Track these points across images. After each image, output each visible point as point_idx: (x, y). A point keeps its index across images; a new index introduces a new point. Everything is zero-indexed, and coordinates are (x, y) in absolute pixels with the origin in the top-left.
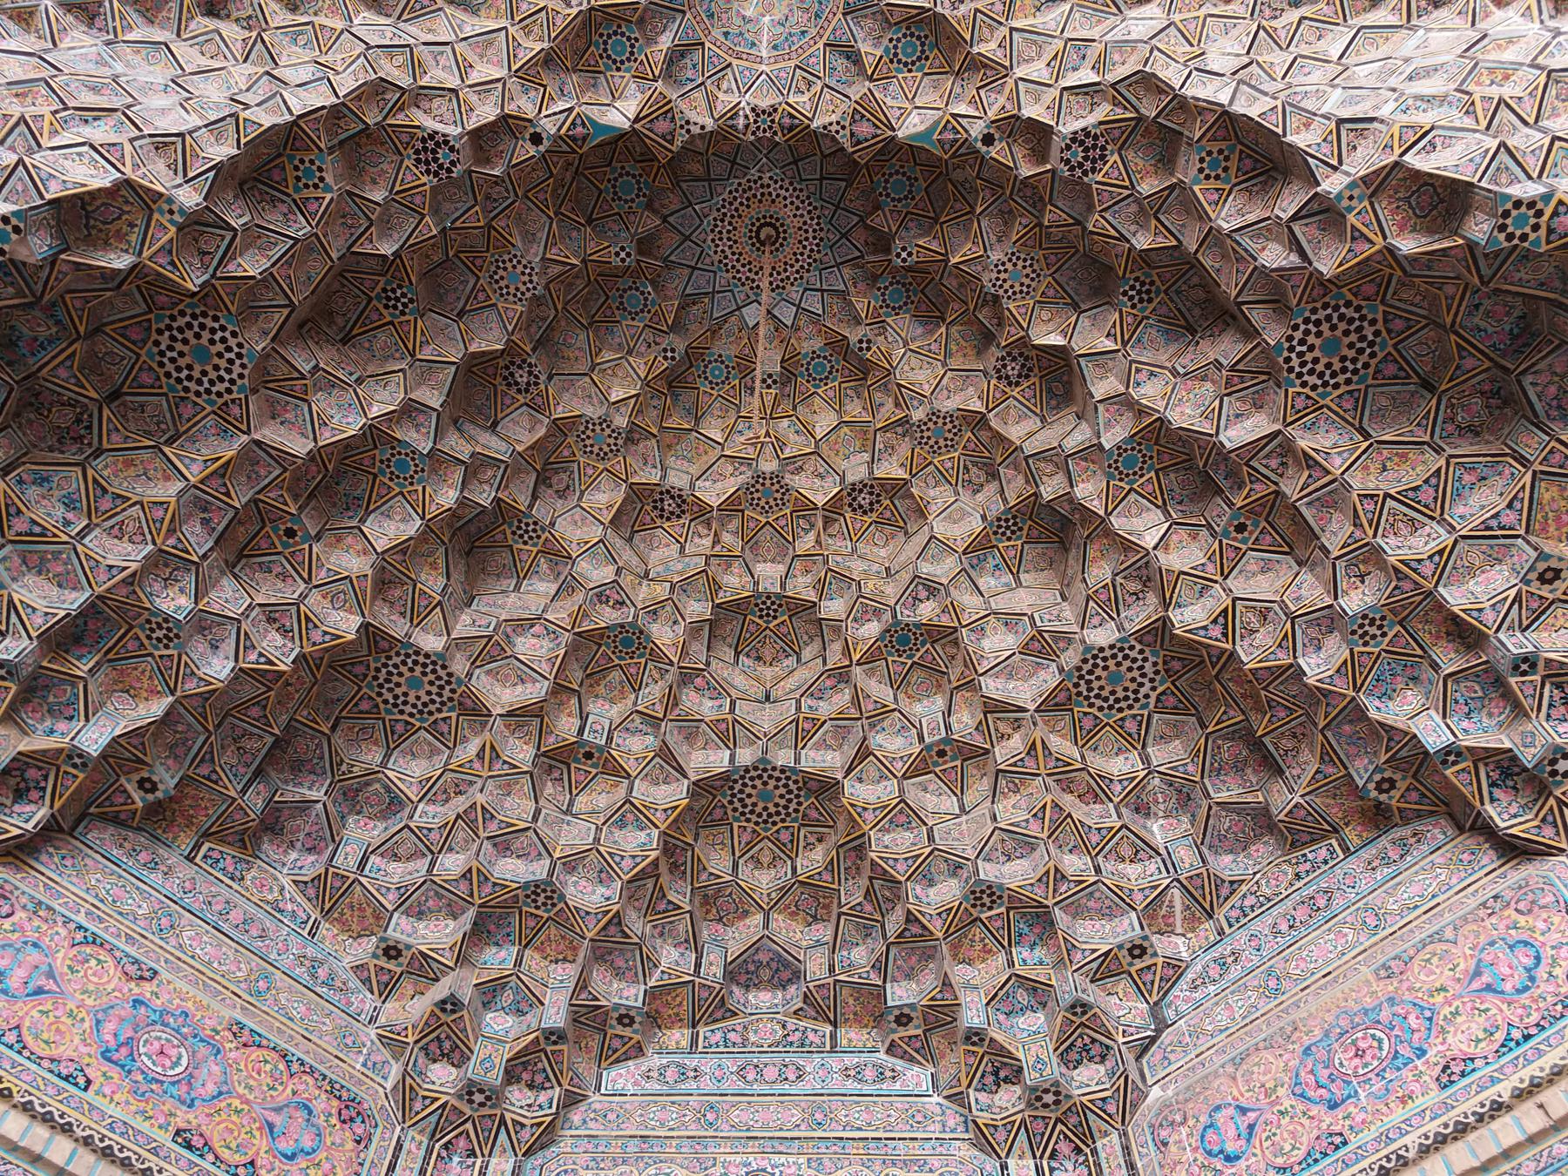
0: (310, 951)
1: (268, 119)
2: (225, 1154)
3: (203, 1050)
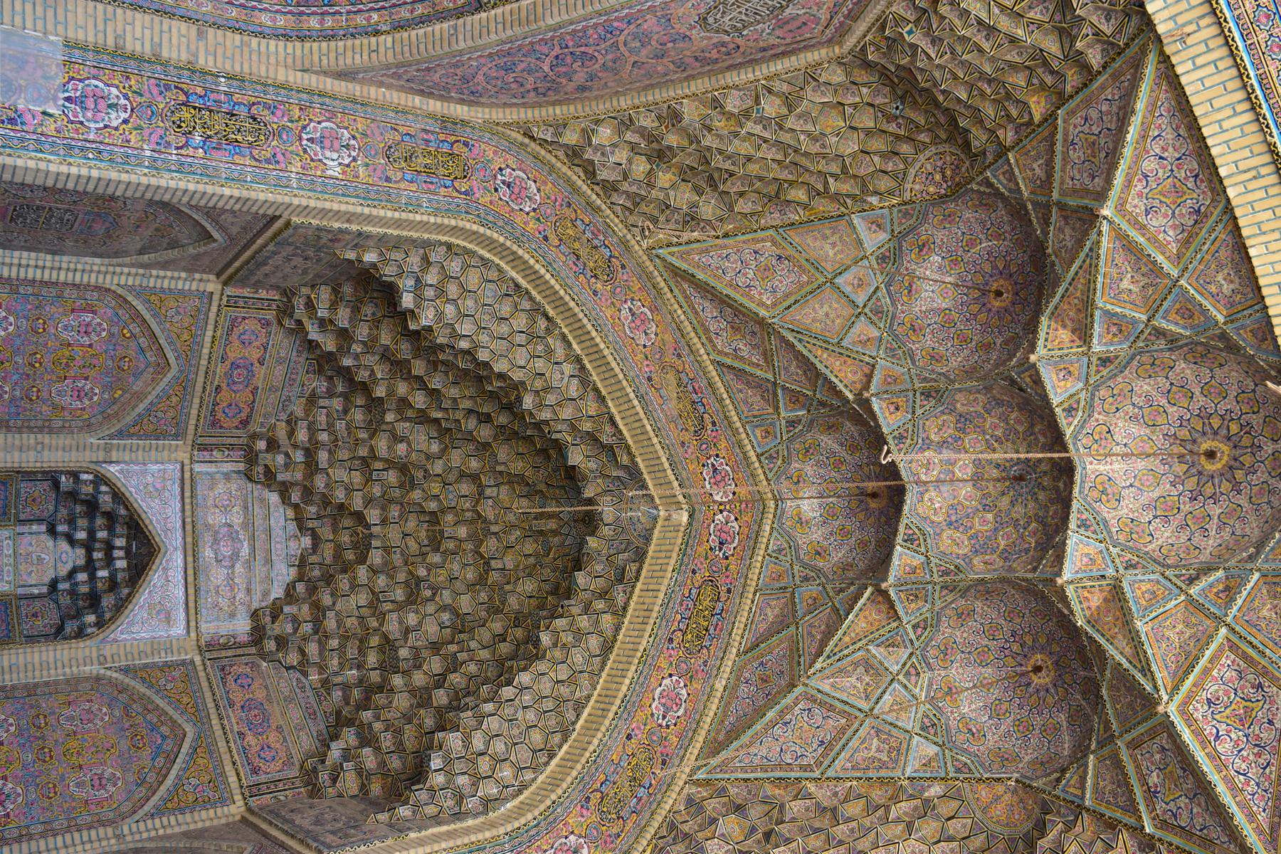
1: (483, 356)
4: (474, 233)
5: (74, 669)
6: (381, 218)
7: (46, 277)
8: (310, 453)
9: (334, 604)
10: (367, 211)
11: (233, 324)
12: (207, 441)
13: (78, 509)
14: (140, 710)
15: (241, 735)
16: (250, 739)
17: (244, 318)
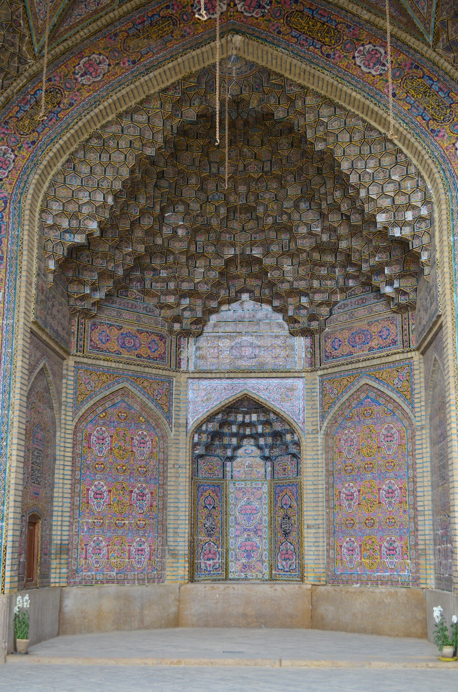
0: (145, 306)
1: (118, 186)
2: (144, 356)
3: (135, 338)
4: (33, 196)
5: (319, 448)
6: (28, 262)
7: (70, 463)
8: (184, 295)
9: (289, 282)
10: (24, 273)
11: (95, 347)
12: (173, 362)
13: (217, 443)
14: (349, 410)
15: (371, 349)
16: (373, 344)
17: (91, 340)
